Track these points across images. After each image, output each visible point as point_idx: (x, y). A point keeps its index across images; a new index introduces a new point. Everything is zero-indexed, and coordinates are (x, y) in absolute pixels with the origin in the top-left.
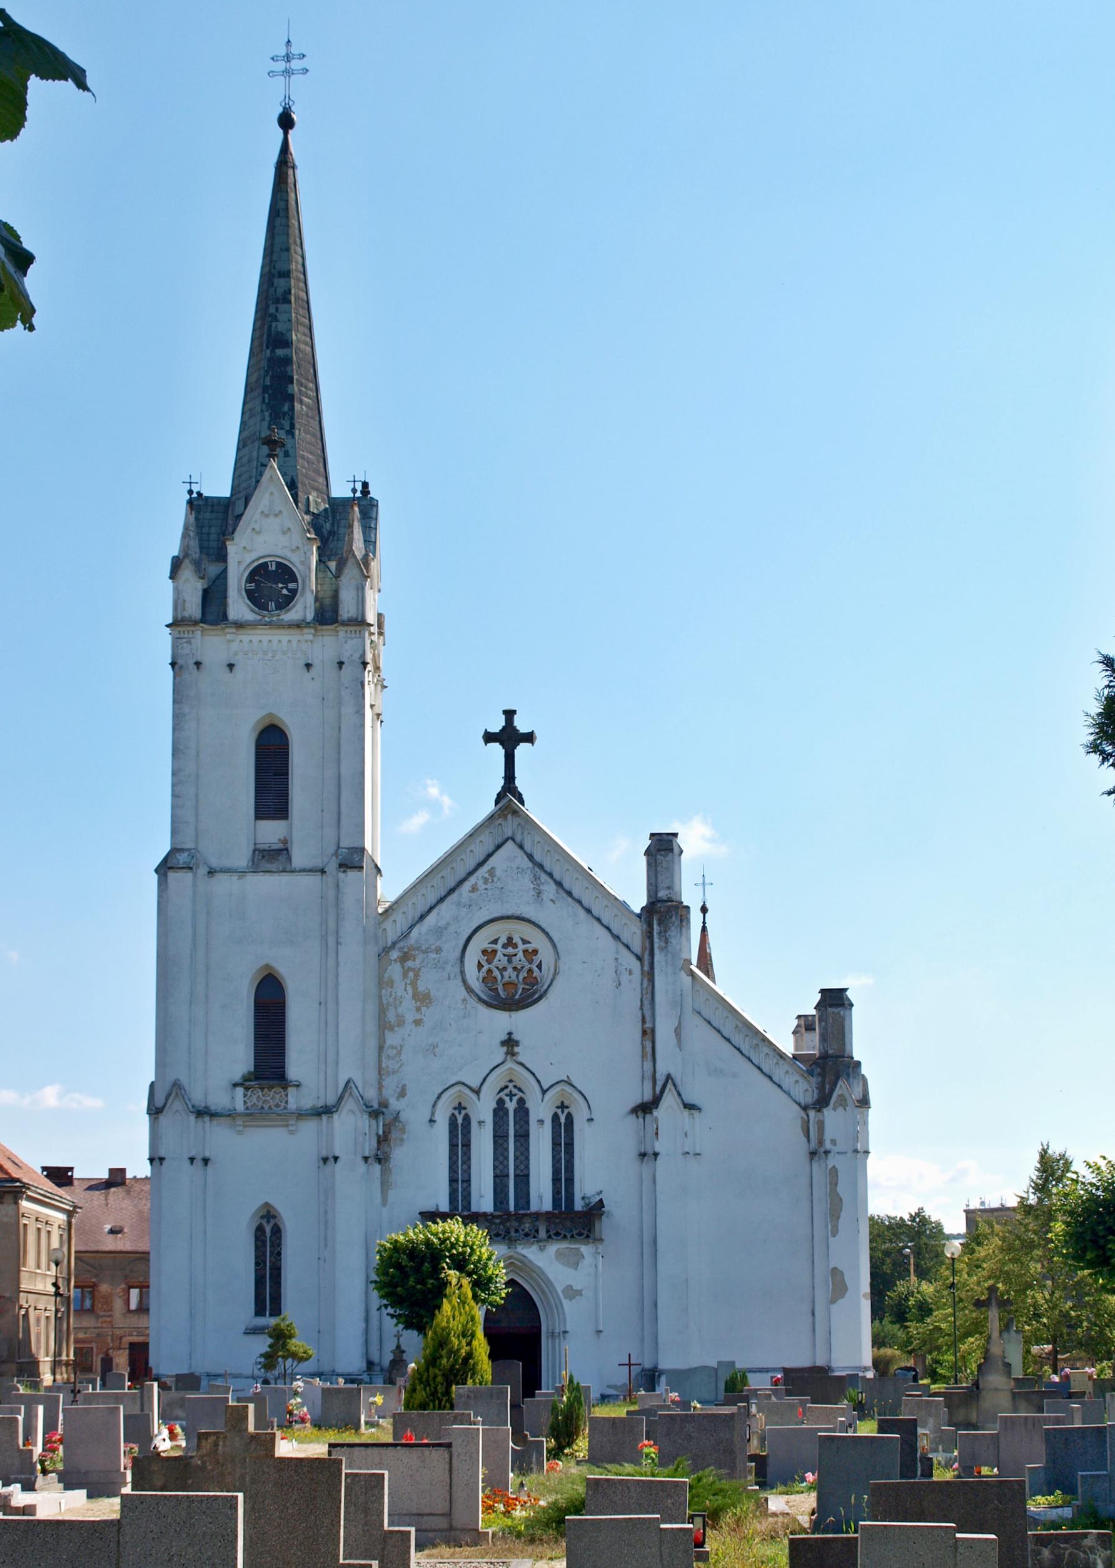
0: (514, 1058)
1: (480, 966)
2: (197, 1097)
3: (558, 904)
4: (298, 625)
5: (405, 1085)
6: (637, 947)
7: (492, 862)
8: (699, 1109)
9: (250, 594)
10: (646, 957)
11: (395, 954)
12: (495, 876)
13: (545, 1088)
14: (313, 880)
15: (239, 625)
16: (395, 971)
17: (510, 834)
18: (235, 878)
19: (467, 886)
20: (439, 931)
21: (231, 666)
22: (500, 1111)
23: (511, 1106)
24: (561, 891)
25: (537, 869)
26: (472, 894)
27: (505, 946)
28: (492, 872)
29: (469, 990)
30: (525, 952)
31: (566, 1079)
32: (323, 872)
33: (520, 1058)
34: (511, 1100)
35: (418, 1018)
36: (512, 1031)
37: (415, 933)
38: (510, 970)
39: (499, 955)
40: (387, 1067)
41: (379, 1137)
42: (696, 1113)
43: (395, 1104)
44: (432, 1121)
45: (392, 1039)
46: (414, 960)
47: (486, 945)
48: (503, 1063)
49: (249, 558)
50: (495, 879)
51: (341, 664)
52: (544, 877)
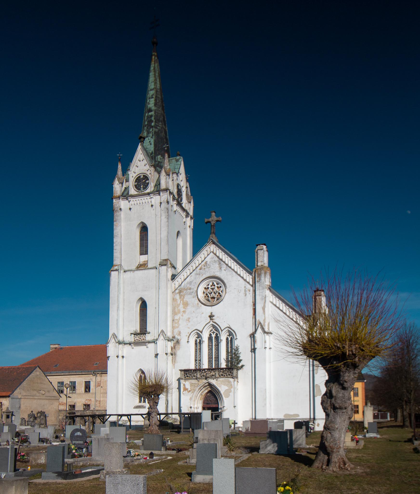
0: (213, 320)
1: (204, 293)
2: (120, 338)
3: (226, 271)
4: (149, 194)
5: (180, 331)
6: (251, 283)
7: (206, 260)
8: (271, 333)
9: (136, 186)
10: (254, 285)
11: (177, 291)
12: (207, 264)
13: (222, 329)
14: (154, 271)
15: (133, 196)
16: (178, 297)
17: (212, 251)
18: (132, 272)
19: (199, 268)
20: (190, 283)
21: (130, 209)
22: (210, 338)
23: (214, 336)
24: (227, 267)
25: (220, 260)
26: (200, 270)
27: (211, 286)
28: (206, 263)
29: (199, 300)
30: (218, 287)
31: (229, 326)
32: (156, 268)
33: (215, 321)
34: (213, 334)
35: (184, 310)
36: (212, 312)
37: (183, 284)
38: (213, 293)
39: (210, 289)
40: (175, 326)
41: (172, 347)
42: (270, 335)
43: (176, 336)
44: (188, 342)
45: (177, 317)
46: (183, 293)
47: (205, 286)
48: (209, 322)
49: (135, 175)
50: (207, 265)
51: (161, 203)
52: (222, 263)
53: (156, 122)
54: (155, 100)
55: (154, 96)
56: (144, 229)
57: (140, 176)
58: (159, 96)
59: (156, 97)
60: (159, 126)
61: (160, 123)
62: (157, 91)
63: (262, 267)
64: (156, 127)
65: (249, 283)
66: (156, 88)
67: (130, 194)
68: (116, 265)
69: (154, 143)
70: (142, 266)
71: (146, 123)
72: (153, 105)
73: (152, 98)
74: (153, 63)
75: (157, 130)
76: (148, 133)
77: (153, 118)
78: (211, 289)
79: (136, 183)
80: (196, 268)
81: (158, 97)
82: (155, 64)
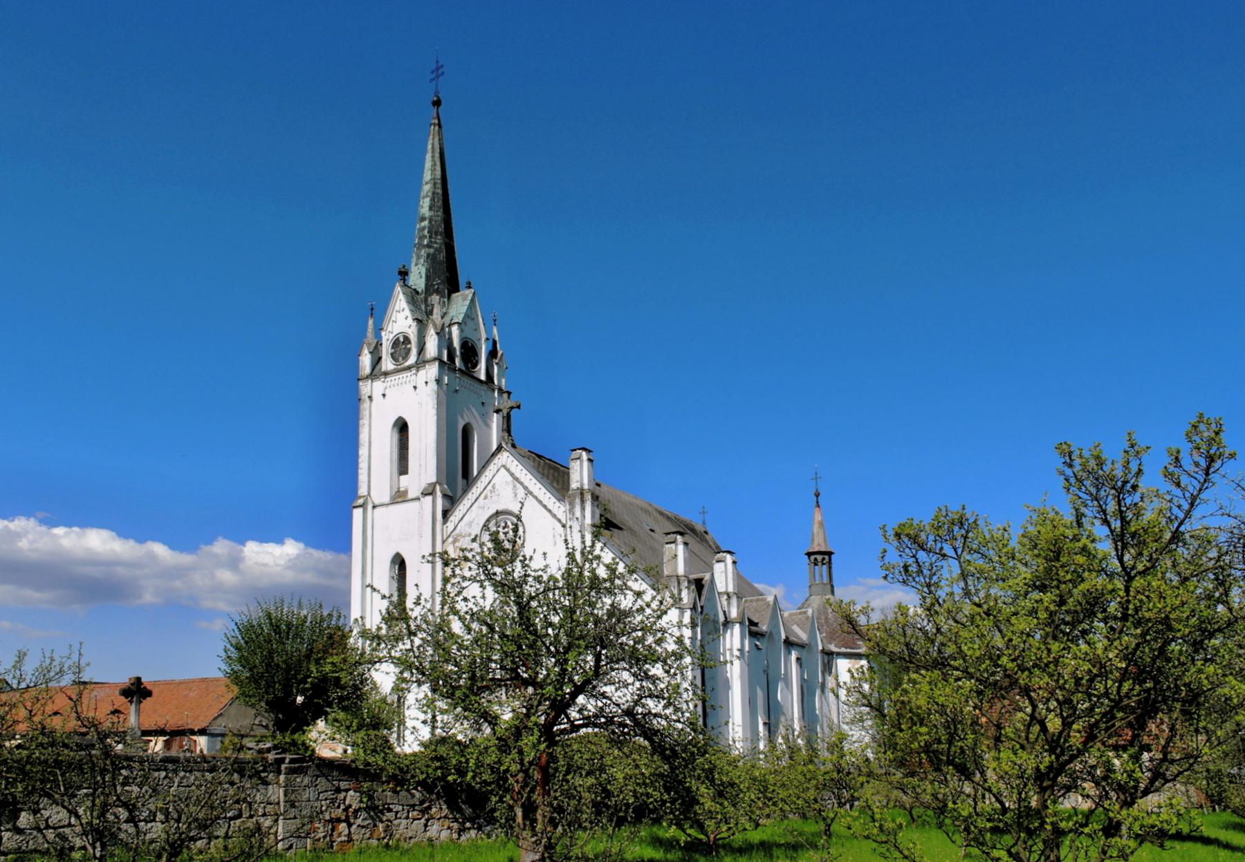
4: (409, 368)
9: (392, 354)
11: (450, 540)
14: (416, 504)
15: (386, 374)
19: (483, 496)
20: (470, 524)
28: (494, 487)
49: (391, 336)
51: (426, 383)
52: (518, 485)
53: (430, 237)
54: (431, 200)
55: (430, 194)
56: (402, 427)
57: (398, 339)
58: (440, 191)
59: (433, 193)
60: (436, 243)
61: (439, 237)
62: (435, 184)
63: (582, 492)
64: (429, 246)
65: (559, 521)
66: (434, 179)
67: (383, 370)
68: (361, 497)
69: (427, 275)
70: (399, 497)
71: (416, 242)
72: (428, 209)
73: (427, 196)
74: (431, 137)
75: (432, 251)
76: (419, 257)
77: (426, 232)
78: (504, 533)
79: (393, 350)
80: (480, 495)
81: (438, 194)
82: (433, 139)
